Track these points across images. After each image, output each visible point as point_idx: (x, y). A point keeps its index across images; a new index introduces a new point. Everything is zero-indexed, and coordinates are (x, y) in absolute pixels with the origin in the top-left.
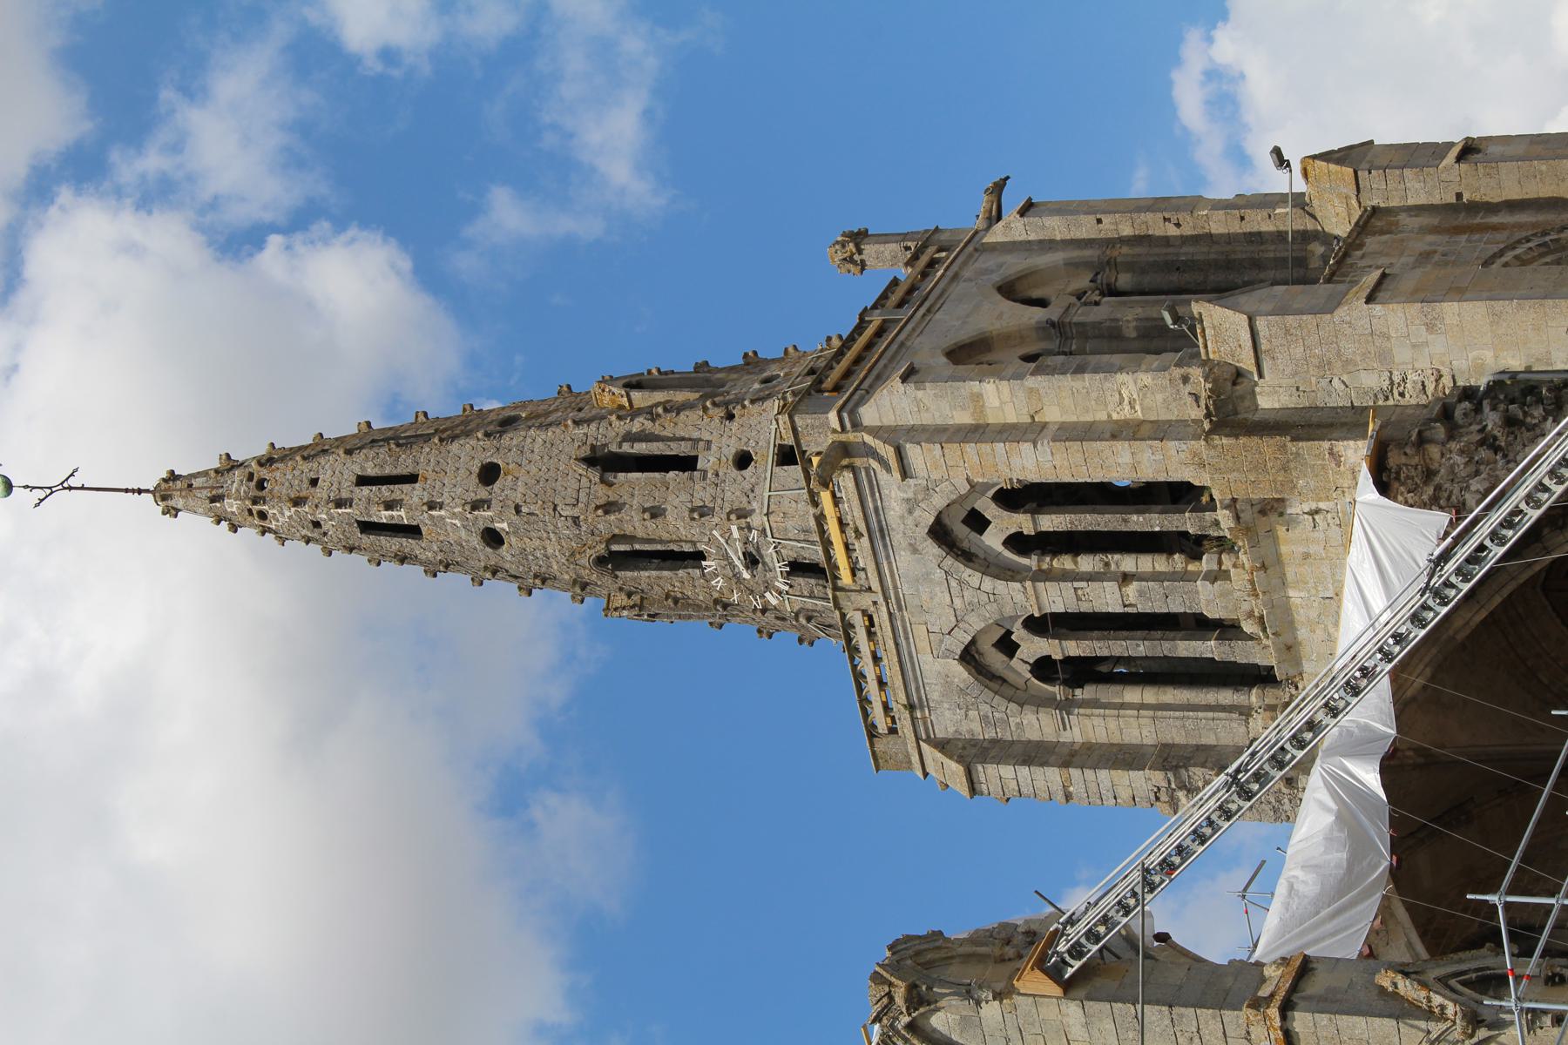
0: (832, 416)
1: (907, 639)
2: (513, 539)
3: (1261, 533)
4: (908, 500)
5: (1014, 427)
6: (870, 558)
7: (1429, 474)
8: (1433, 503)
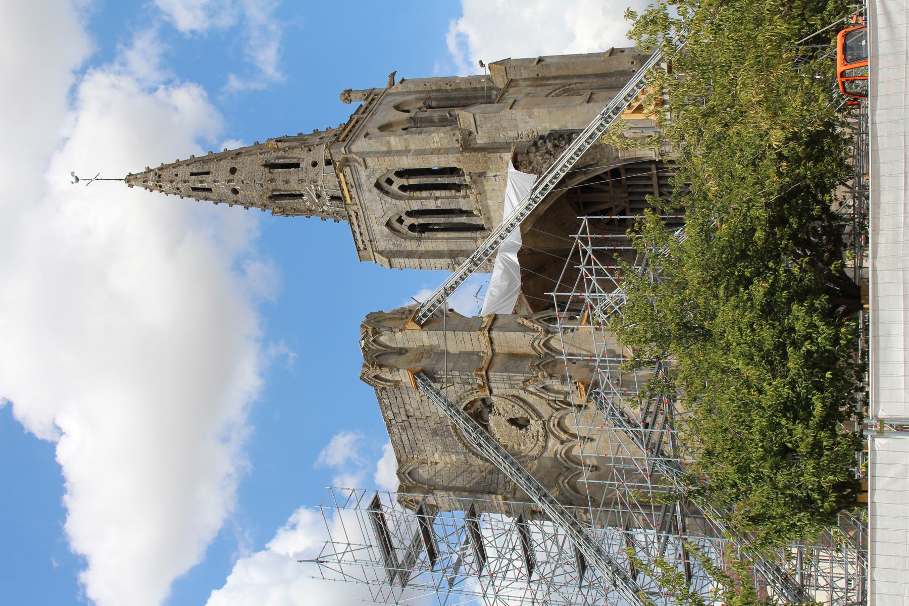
0: (343, 149)
2: (242, 192)
3: (479, 182)
4: (367, 175)
5: (400, 151)
6: (356, 194)
7: (531, 163)
8: (532, 172)
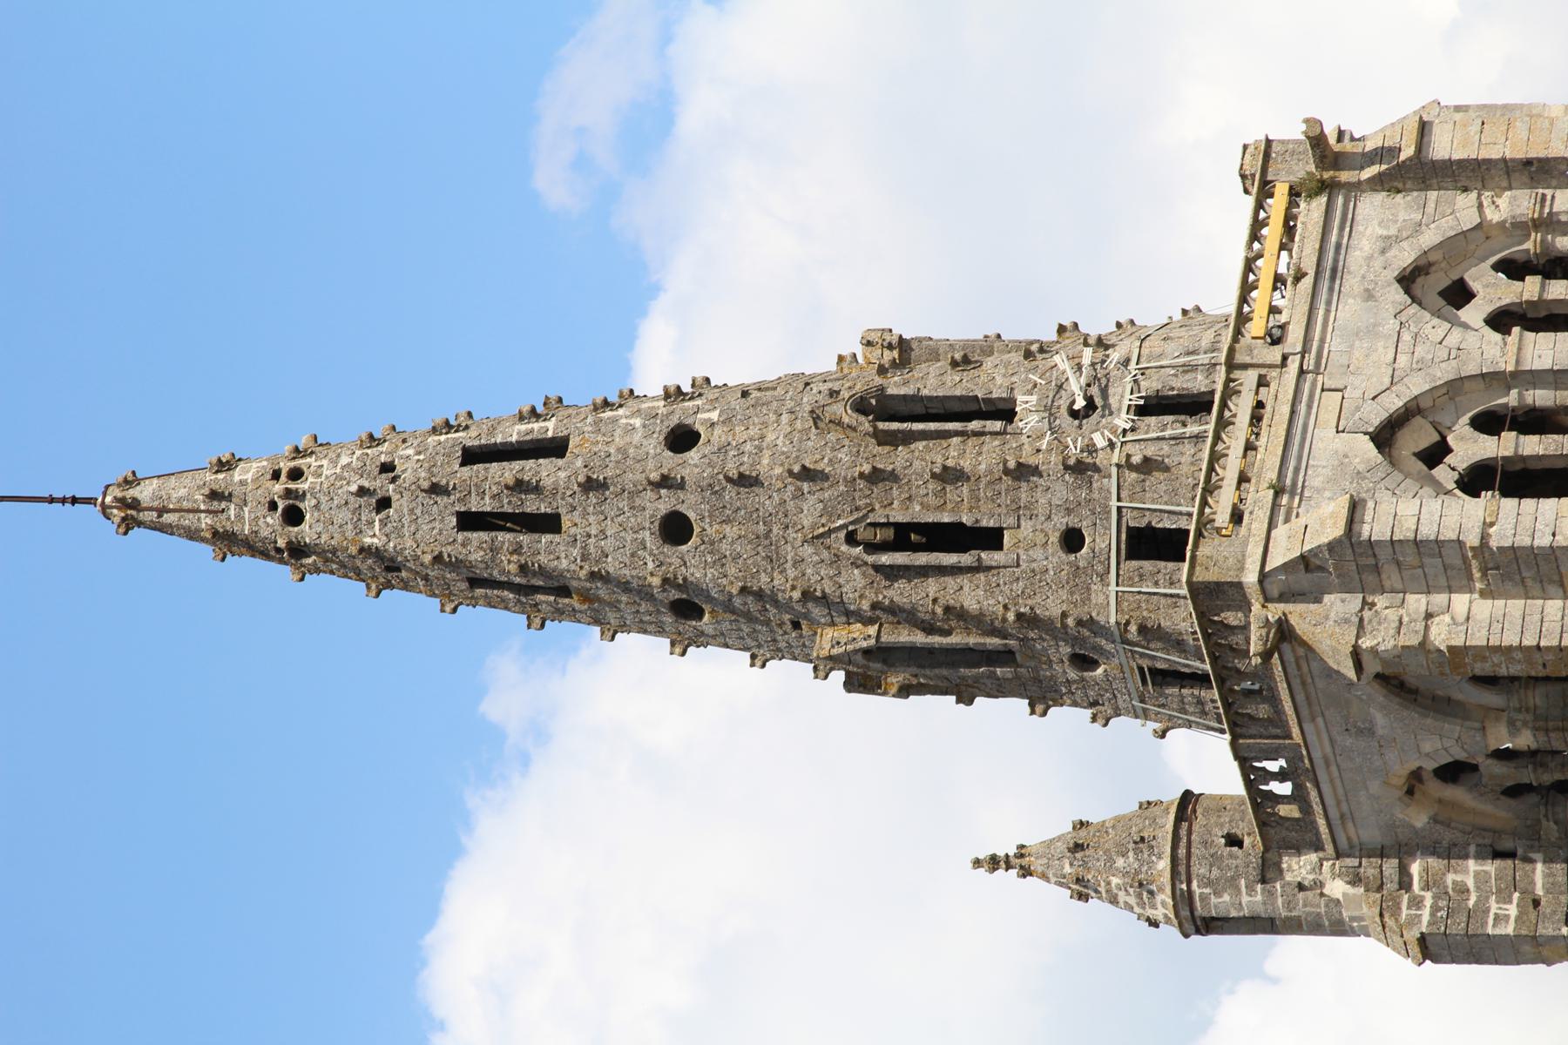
1: (1309, 407)
